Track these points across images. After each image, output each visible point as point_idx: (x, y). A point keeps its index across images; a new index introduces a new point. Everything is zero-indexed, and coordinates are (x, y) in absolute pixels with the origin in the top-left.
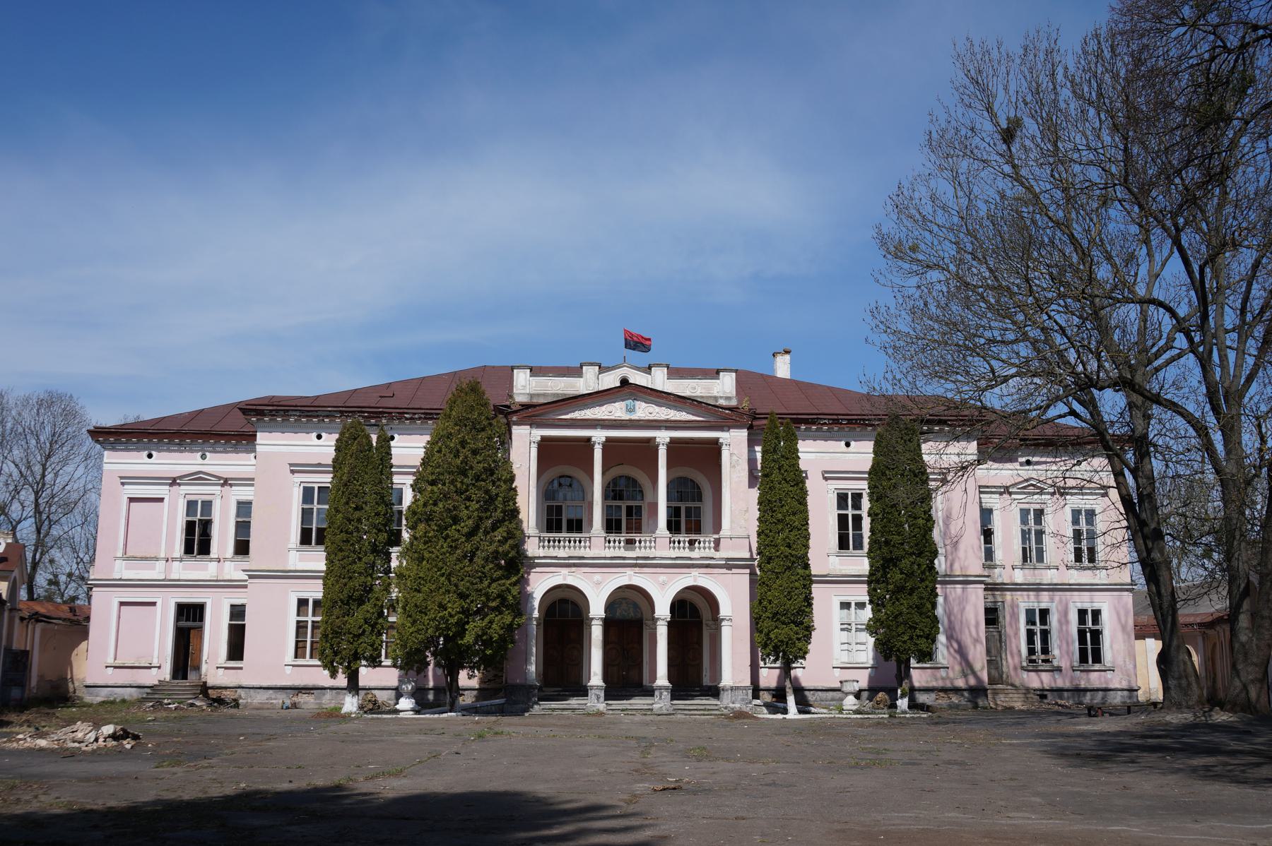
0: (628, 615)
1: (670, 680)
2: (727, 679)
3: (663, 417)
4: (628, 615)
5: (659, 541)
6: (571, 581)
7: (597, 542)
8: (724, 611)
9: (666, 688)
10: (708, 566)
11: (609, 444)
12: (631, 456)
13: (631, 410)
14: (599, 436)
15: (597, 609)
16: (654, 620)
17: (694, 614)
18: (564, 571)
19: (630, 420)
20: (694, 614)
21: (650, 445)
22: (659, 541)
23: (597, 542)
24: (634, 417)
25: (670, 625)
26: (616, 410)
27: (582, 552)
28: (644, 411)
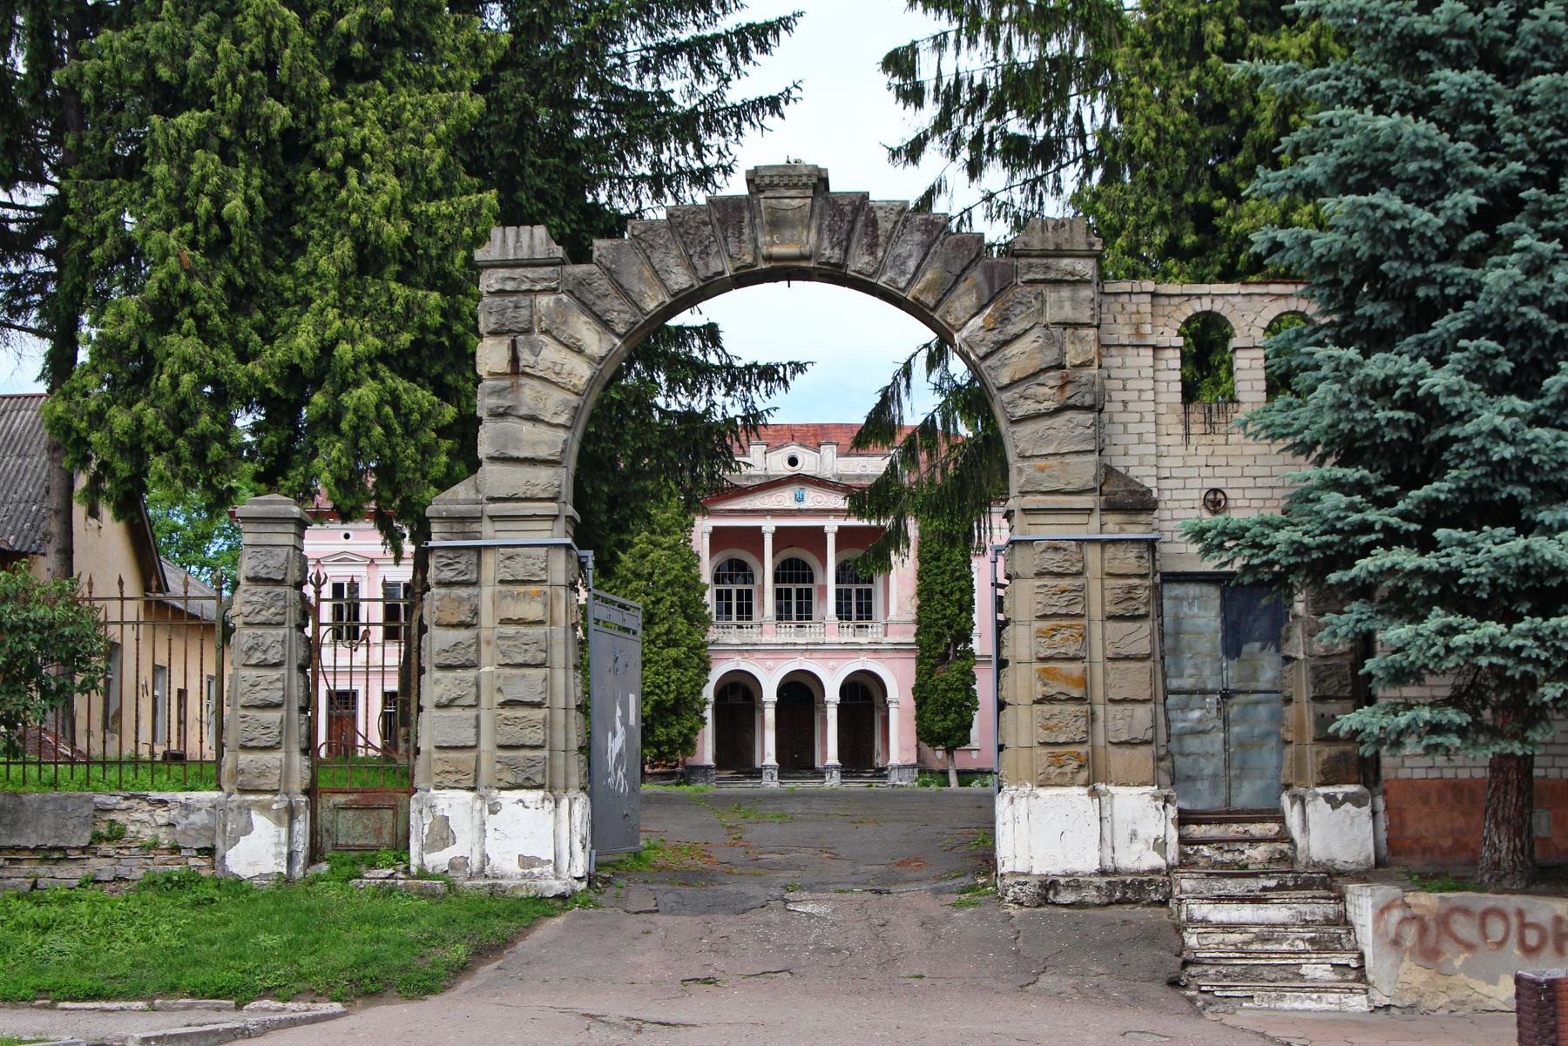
0: (800, 693)
1: (840, 758)
2: (895, 758)
3: (832, 506)
4: (800, 693)
5: (827, 623)
6: (744, 666)
7: (767, 627)
8: (893, 692)
9: (836, 767)
10: (875, 651)
11: (780, 533)
12: (798, 547)
13: (800, 499)
14: (769, 525)
15: (770, 694)
16: (824, 704)
17: (863, 695)
18: (738, 658)
19: (799, 510)
20: (863, 695)
21: (819, 533)
22: (827, 623)
23: (767, 627)
24: (803, 506)
25: (840, 708)
26: (784, 499)
27: (755, 639)
28: (815, 498)
